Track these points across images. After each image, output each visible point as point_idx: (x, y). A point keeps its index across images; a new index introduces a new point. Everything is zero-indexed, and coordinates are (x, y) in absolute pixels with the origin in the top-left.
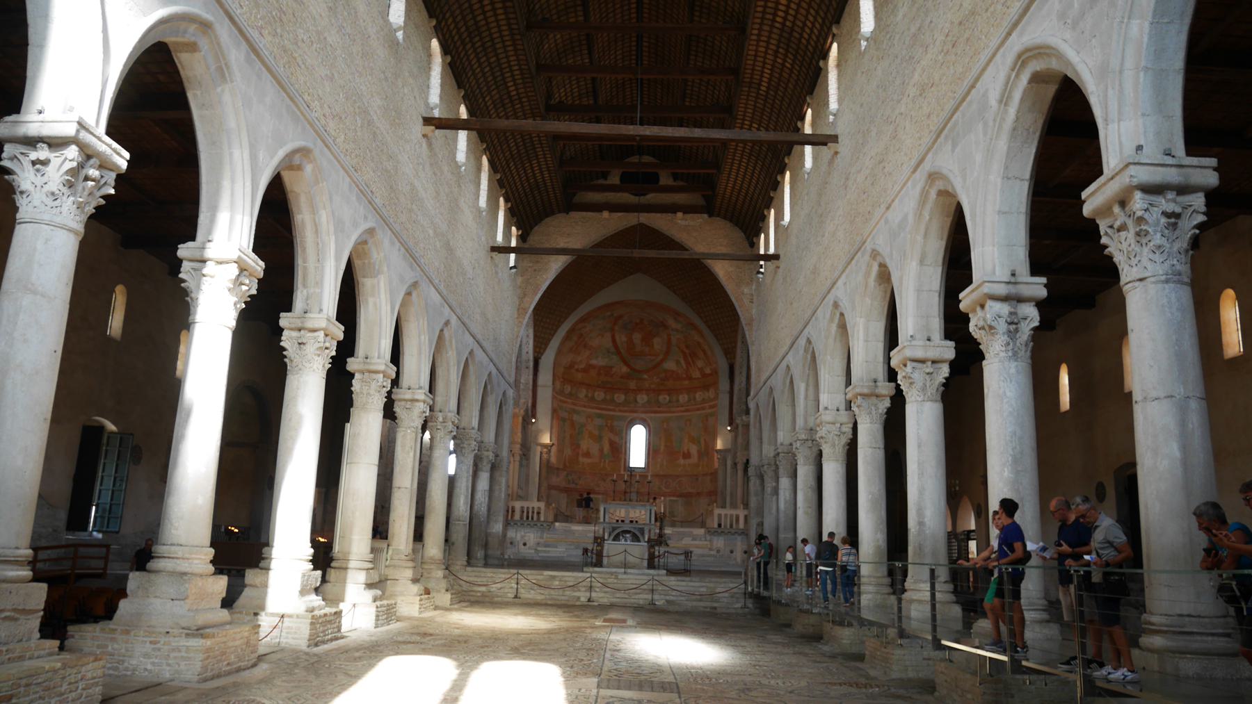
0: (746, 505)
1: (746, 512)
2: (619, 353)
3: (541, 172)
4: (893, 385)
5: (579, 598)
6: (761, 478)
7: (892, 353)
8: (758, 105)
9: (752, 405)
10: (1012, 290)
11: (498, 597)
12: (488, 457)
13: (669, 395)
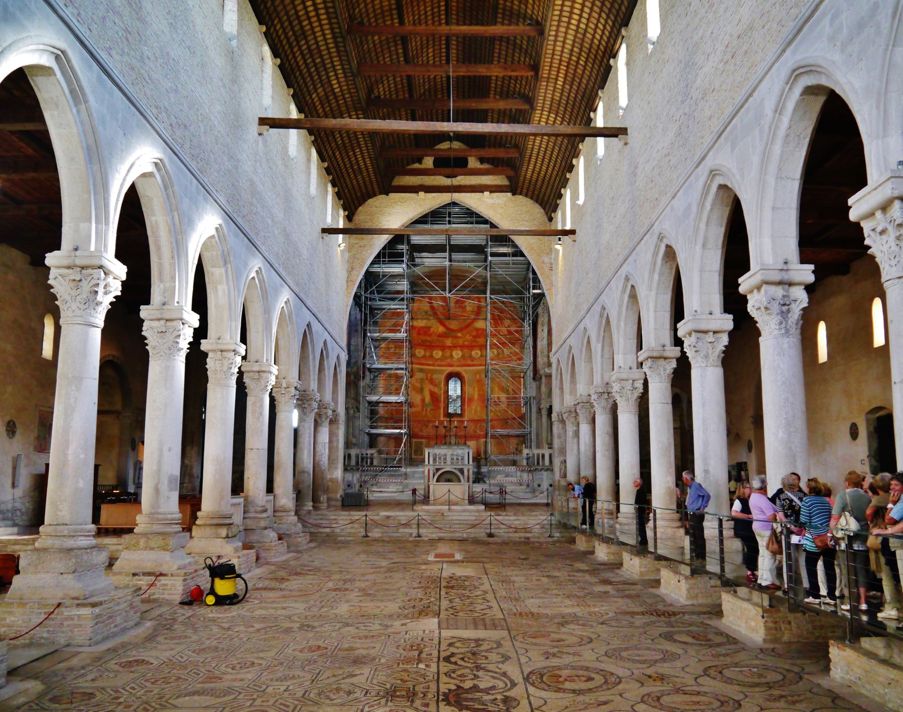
0: (550, 446)
1: (550, 451)
2: (435, 314)
3: (364, 159)
4: (679, 348)
5: (411, 535)
6: (563, 422)
7: (679, 325)
8: (555, 97)
9: (553, 360)
10: (785, 277)
11: (341, 536)
12: (326, 414)
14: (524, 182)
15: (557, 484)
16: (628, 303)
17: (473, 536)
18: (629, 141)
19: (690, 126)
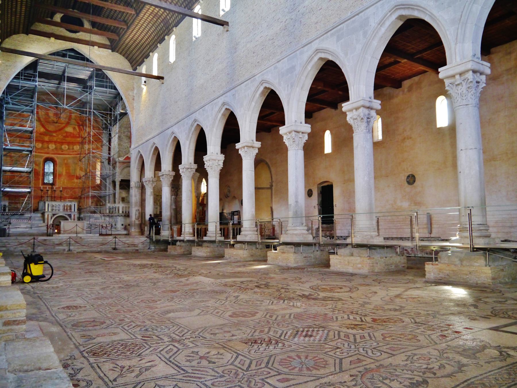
5: (64, 250)
13: (68, 145)
14: (123, 44)
15: (133, 223)
16: (220, 118)
17: (104, 250)
18: (229, 30)
19: (296, 26)
